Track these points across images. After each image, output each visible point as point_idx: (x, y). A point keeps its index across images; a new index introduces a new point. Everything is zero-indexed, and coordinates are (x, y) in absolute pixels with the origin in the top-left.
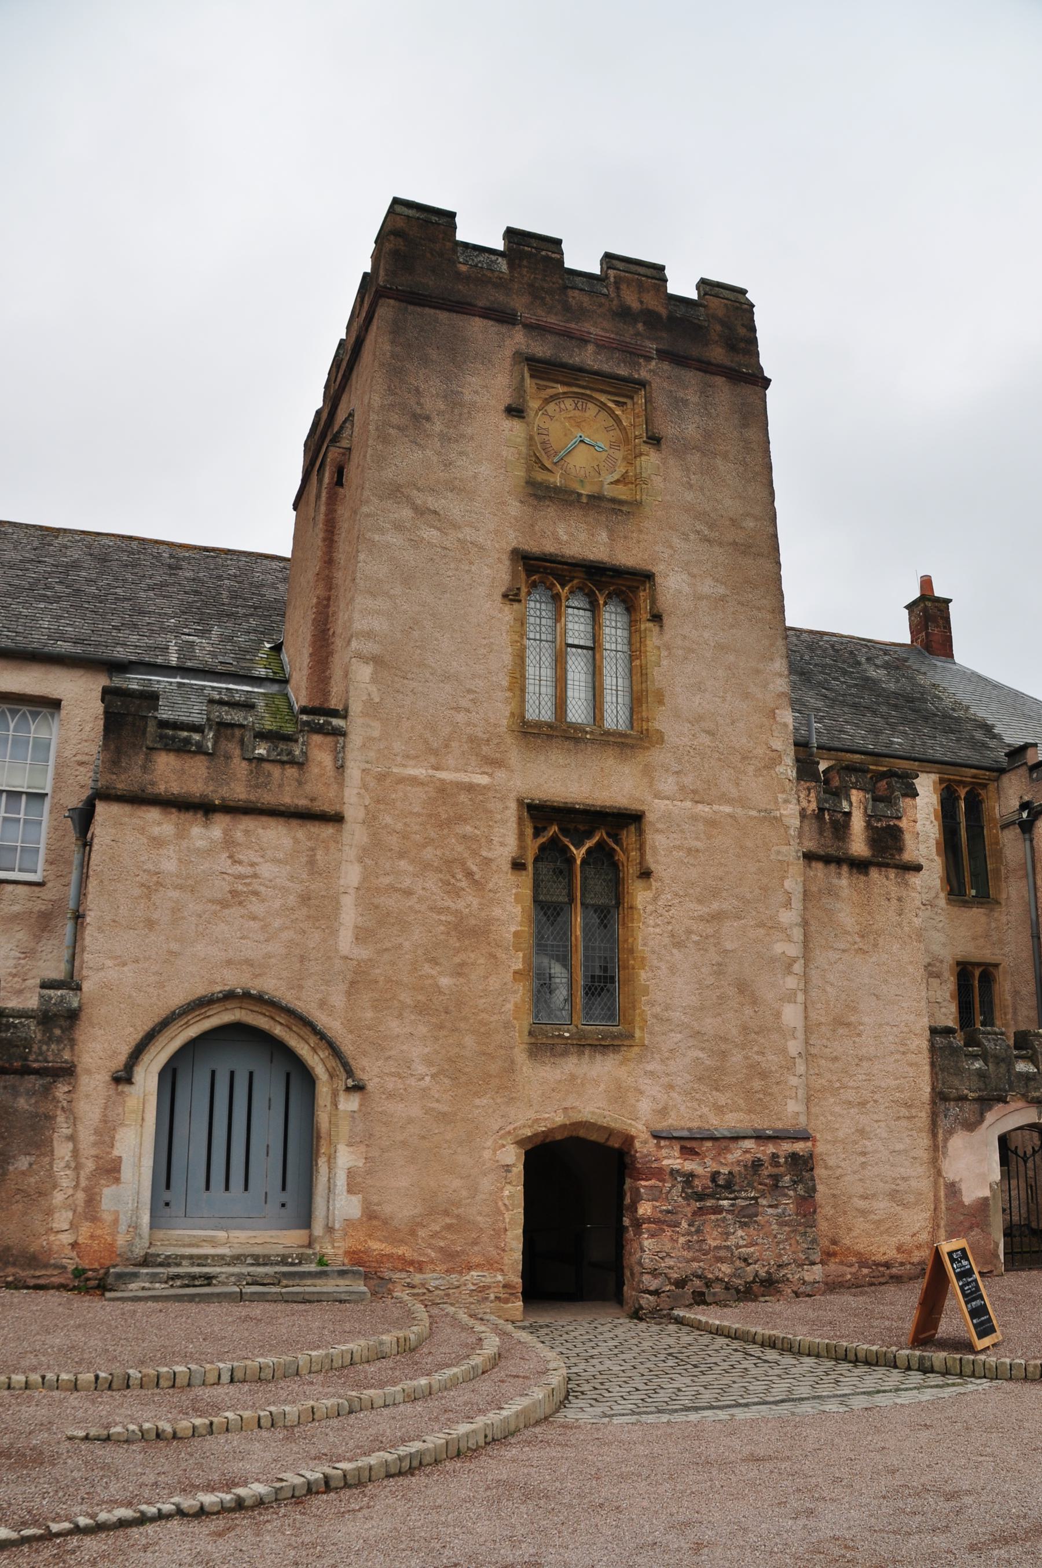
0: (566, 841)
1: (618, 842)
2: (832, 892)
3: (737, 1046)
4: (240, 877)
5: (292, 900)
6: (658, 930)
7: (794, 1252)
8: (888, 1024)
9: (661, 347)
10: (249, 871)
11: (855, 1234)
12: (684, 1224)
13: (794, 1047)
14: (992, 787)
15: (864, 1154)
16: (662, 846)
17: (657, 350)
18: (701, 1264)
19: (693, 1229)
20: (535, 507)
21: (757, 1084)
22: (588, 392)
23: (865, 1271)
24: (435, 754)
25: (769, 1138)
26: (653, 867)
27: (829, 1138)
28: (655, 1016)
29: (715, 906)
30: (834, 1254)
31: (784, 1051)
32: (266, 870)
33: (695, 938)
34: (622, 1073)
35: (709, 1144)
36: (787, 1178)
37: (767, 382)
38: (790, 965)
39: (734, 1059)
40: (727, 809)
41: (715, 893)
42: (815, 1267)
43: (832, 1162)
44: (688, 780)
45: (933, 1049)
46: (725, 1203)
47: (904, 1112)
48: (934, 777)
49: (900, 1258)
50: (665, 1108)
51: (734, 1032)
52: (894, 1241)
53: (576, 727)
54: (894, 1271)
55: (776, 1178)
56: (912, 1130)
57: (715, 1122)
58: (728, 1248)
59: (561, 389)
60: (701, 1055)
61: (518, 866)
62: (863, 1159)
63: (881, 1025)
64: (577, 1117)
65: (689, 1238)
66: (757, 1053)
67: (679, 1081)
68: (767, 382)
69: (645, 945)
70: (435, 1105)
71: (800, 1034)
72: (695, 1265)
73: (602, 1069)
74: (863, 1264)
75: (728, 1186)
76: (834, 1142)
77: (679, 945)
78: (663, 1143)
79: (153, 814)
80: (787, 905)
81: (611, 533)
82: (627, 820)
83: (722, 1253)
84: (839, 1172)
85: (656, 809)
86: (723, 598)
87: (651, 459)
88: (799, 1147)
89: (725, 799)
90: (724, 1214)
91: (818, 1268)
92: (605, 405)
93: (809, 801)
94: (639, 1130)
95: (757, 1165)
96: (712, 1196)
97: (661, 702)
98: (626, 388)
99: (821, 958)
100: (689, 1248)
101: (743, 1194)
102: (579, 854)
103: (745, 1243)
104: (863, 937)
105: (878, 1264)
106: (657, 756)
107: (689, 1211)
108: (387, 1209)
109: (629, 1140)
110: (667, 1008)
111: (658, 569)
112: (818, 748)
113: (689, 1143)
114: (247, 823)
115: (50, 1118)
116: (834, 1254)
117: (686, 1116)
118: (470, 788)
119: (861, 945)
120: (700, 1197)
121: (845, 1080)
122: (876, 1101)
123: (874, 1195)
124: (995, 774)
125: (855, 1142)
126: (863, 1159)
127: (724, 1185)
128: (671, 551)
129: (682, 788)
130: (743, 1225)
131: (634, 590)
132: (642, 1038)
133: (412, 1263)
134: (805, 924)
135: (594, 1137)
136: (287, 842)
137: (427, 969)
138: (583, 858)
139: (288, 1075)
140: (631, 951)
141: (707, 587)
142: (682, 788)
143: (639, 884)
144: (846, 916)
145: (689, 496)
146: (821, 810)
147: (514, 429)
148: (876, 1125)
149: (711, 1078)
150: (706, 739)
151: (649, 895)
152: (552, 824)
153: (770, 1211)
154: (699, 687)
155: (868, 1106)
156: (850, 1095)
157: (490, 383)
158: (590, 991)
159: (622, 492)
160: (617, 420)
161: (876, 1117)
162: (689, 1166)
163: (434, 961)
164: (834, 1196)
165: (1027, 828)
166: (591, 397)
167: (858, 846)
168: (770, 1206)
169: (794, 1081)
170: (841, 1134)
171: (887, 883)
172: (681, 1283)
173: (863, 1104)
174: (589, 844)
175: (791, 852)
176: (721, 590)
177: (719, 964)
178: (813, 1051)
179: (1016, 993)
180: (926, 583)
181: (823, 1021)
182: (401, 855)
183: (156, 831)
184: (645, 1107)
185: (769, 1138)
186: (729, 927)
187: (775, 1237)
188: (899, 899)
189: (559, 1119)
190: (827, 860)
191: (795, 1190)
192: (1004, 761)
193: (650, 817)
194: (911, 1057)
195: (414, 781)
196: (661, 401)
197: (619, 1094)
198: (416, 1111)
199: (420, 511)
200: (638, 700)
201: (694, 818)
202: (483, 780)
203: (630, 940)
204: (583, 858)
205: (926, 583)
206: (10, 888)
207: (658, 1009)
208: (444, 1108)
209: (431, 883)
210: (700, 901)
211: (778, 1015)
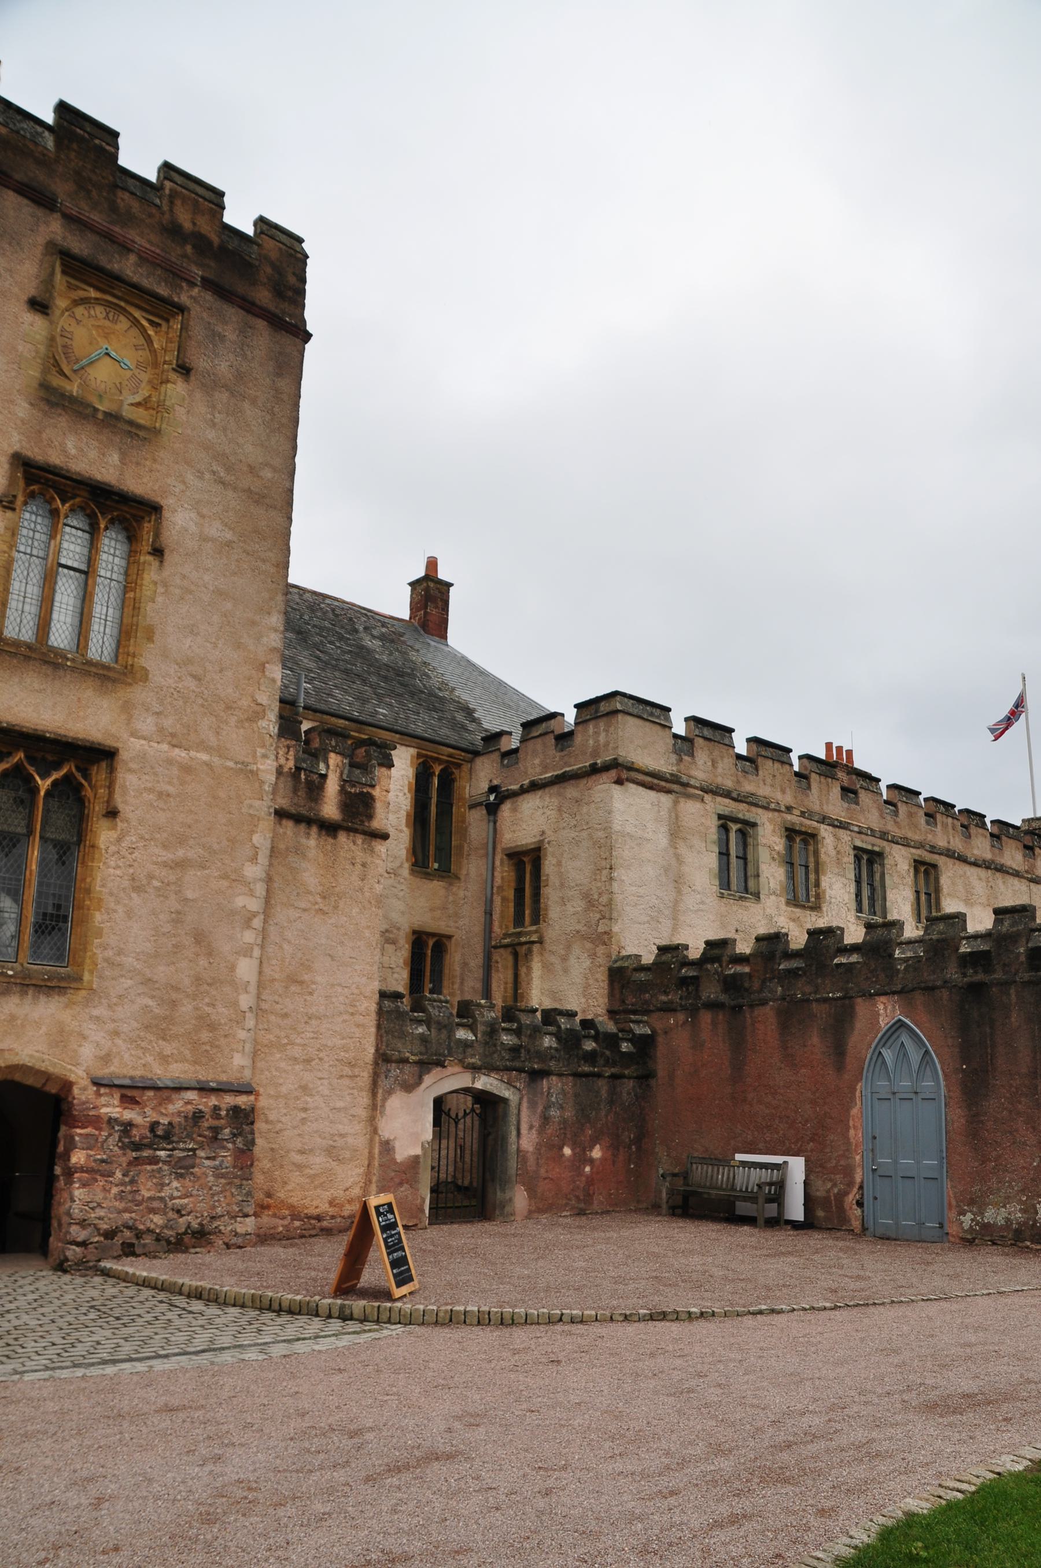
0: (32, 770)
1: (86, 776)
2: (299, 851)
3: (188, 996)
6: (118, 872)
7: (228, 1204)
8: (340, 985)
9: (207, 275)
11: (289, 1187)
12: (119, 1174)
13: (246, 1001)
14: (466, 767)
15: (305, 1110)
16: (131, 786)
17: (203, 278)
18: (133, 1215)
19: (127, 1179)
20: (45, 413)
21: (205, 1035)
22: (122, 304)
23: (297, 1223)
25: (213, 1090)
26: (121, 807)
27: (272, 1093)
28: (106, 960)
29: (180, 853)
30: (268, 1207)
31: (235, 1004)
33: (156, 883)
34: (66, 1016)
35: (151, 1093)
36: (227, 1131)
37: (308, 336)
38: (250, 920)
39: (184, 1009)
40: (204, 757)
41: (182, 840)
42: (247, 1220)
43: (272, 1117)
44: (168, 722)
45: (380, 1012)
46: (162, 1153)
47: (347, 1071)
48: (413, 751)
49: (332, 1211)
50: (108, 1055)
51: (187, 981)
52: (327, 1195)
53: (57, 652)
54: (325, 1224)
55: (216, 1130)
56: (353, 1088)
57: (159, 1072)
58: (161, 1199)
59: (93, 293)
60: (150, 1002)
62: (304, 1115)
63: (333, 985)
64: (14, 1060)
65: (122, 1188)
66: (208, 1005)
67: (125, 1028)
68: (308, 336)
69: (103, 886)
71: (253, 989)
72: (127, 1216)
73: (46, 1010)
74: (295, 1217)
75: (167, 1137)
76: (277, 1097)
77: (138, 889)
78: (102, 1090)
80: (254, 859)
81: (123, 456)
82: (99, 756)
83: (156, 1204)
84: (279, 1126)
85: (130, 748)
86: (229, 544)
87: (177, 389)
88: (242, 1100)
89: (202, 746)
90: (161, 1165)
91: (250, 1221)
92: (138, 321)
93: (287, 759)
95: (198, 1116)
96: (149, 1146)
97: (150, 639)
98: (163, 309)
99: (281, 914)
100: (122, 1199)
101: (181, 1145)
102: (44, 785)
103: (179, 1194)
104: (324, 898)
105: (309, 1217)
106: (139, 694)
107: (124, 1161)
109: (67, 1086)
110: (120, 952)
112: (305, 708)
113: (130, 1092)
116: (268, 1207)
117: (129, 1064)
119: (321, 906)
120: (137, 1147)
121: (293, 1037)
122: (321, 1059)
123: (311, 1150)
124: (470, 756)
125: (297, 1098)
126: (304, 1115)
127: (162, 1135)
128: (182, 487)
129: (161, 730)
130: (180, 1176)
131: (139, 520)
132: (91, 982)
134: (269, 880)
135: (30, 1081)
140: (88, 891)
141: (215, 530)
142: (161, 730)
143: (104, 823)
144: (311, 876)
145: (211, 434)
146: (298, 769)
147: (35, 324)
148: (319, 1082)
149: (159, 1027)
150: (192, 684)
151: (113, 835)
152: (18, 750)
153: (207, 1163)
154: (192, 631)
155: (313, 1063)
156: (296, 1052)
159: (141, 416)
160: (149, 340)
161: (320, 1075)
162: (128, 1115)
164: (272, 1149)
165: (492, 809)
166: (125, 310)
167: (330, 808)
168: (208, 1158)
169: (242, 1034)
170: (284, 1090)
171: (353, 848)
172: (110, 1235)
173: (308, 1061)
174: (55, 776)
175: (263, 807)
176: (229, 535)
177: (178, 913)
178: (264, 1006)
179: (465, 964)
180: (432, 564)
181: (277, 976)
184: (87, 1052)
185: (213, 1090)
186: (192, 876)
187: (211, 1189)
188: (364, 865)
190: (298, 819)
191: (234, 1143)
193: (124, 755)
194: (359, 1019)
196: (197, 331)
197: (61, 1038)
200: (126, 633)
201: (170, 762)
203: (88, 880)
205: (432, 564)
207: (110, 953)
210: (165, 847)
211: (232, 968)
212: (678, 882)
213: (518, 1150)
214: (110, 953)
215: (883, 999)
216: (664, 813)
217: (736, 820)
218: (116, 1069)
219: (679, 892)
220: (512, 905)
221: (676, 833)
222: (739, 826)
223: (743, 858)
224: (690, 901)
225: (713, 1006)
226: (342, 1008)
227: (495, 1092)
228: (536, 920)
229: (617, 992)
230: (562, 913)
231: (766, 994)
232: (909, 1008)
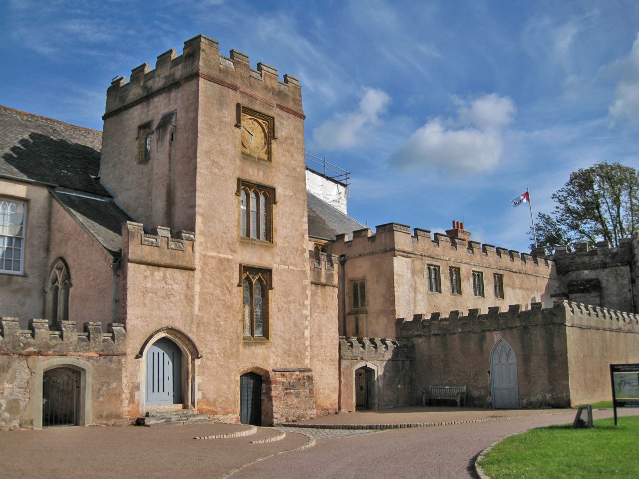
4: (168, 289)
5: (182, 297)
9: (278, 103)
10: (170, 287)
12: (283, 398)
13: (308, 343)
14: (329, 247)
17: (276, 104)
20: (243, 162)
24: (217, 248)
25: (303, 371)
31: (305, 344)
32: (175, 286)
36: (307, 383)
38: (307, 318)
55: (304, 383)
61: (239, 285)
70: (220, 362)
71: (309, 339)
73: (259, 350)
74: (322, 410)
78: (276, 373)
79: (143, 267)
80: (307, 299)
82: (268, 272)
83: (292, 406)
85: (274, 267)
86: (292, 196)
88: (309, 374)
89: (291, 264)
94: (270, 369)
96: (289, 389)
101: (296, 388)
108: (208, 396)
109: (267, 372)
111: (275, 186)
113: (283, 372)
114: (169, 270)
115: (121, 370)
118: (228, 260)
120: (286, 389)
124: (331, 242)
127: (292, 386)
128: (278, 179)
133: (214, 412)
136: (180, 278)
137: (218, 319)
139: (173, 353)
149: (288, 353)
151: (272, 295)
153: (303, 393)
157: (229, 115)
158: (260, 326)
161: (325, 365)
162: (284, 380)
163: (218, 316)
182: (210, 282)
183: (145, 273)
189: (250, 366)
192: (335, 239)
193: (273, 270)
195: (213, 257)
197: (266, 359)
198: (215, 365)
202: (230, 257)
206: (15, 278)
207: (274, 331)
208: (222, 363)
209: (218, 292)
212: (415, 290)
213: (378, 386)
214: (274, 331)
215: (495, 332)
216: (409, 265)
217: (432, 265)
218: (278, 367)
219: (416, 294)
220: (352, 299)
221: (414, 273)
222: (433, 267)
223: (435, 279)
224: (420, 296)
225: (435, 335)
226: (330, 343)
227: (371, 367)
228: (363, 305)
229: (399, 331)
230: (374, 301)
231: (455, 331)
232: (504, 336)
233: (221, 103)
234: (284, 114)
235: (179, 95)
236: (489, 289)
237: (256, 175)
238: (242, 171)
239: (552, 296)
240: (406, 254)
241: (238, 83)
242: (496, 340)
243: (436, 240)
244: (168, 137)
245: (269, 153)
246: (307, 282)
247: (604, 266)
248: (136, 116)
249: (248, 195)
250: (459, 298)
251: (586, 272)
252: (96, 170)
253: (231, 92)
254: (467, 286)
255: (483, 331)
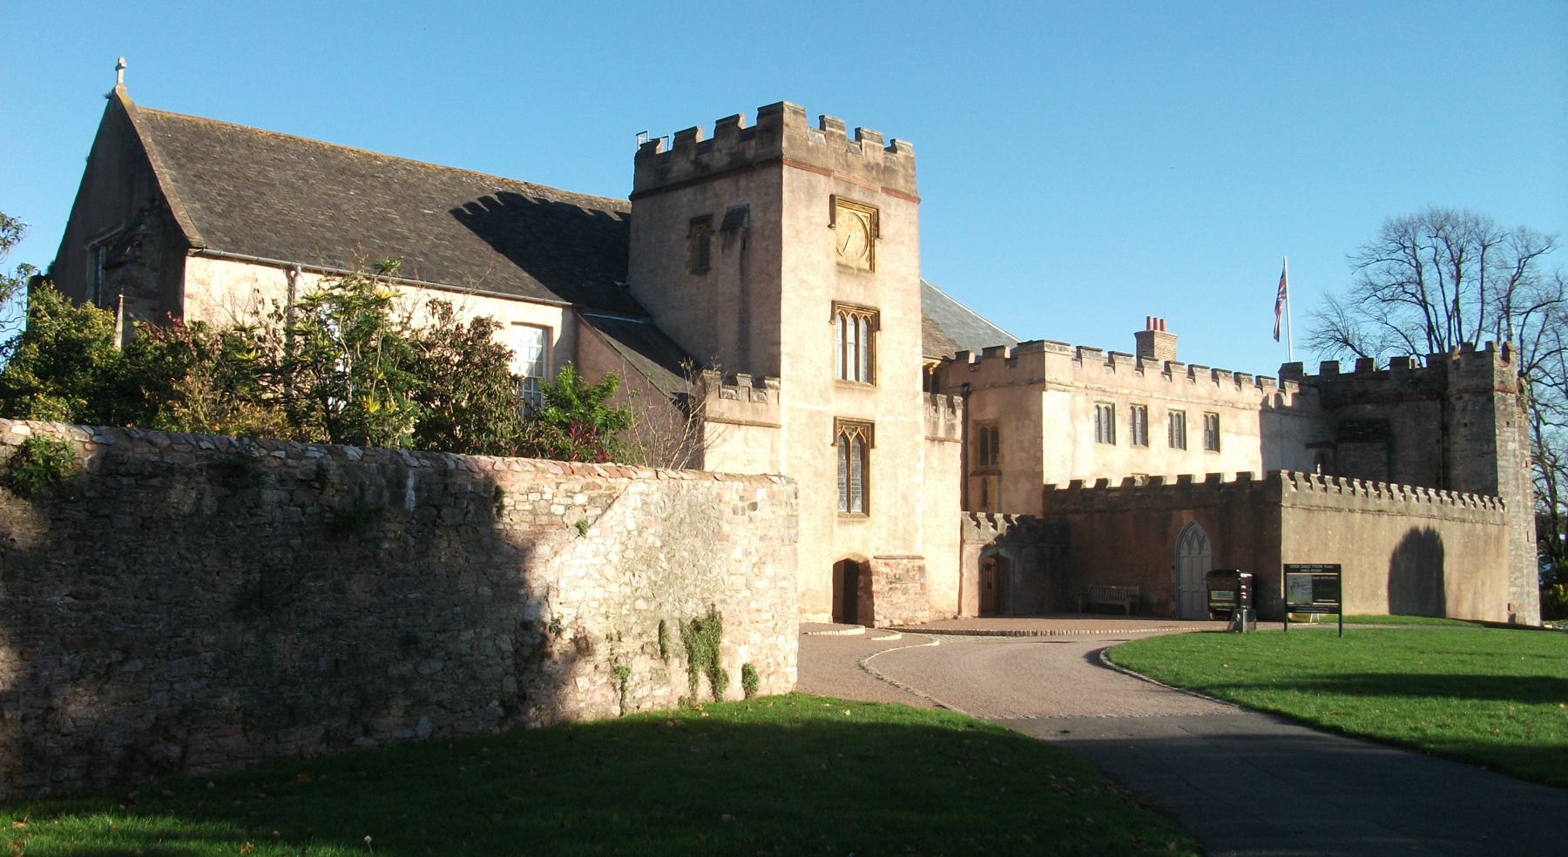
94: (870, 557)
118: (820, 413)
138: (856, 441)
167: (941, 434)
199: (802, 281)
204: (856, 441)
212: (1075, 442)
228: (994, 462)
230: (1010, 457)
233: (811, 194)
234: (893, 200)
235: (753, 185)
236: (1196, 436)
237: (855, 293)
238: (838, 290)
239: (1308, 446)
240: (1063, 388)
241: (831, 163)
242: (1185, 522)
243: (1111, 362)
244: (738, 245)
245: (871, 258)
246: (920, 438)
247: (1399, 398)
248: (687, 203)
249: (844, 322)
250: (1144, 451)
251: (1369, 407)
252: (623, 274)
253: (822, 178)
254: (1159, 432)
255: (1168, 509)
